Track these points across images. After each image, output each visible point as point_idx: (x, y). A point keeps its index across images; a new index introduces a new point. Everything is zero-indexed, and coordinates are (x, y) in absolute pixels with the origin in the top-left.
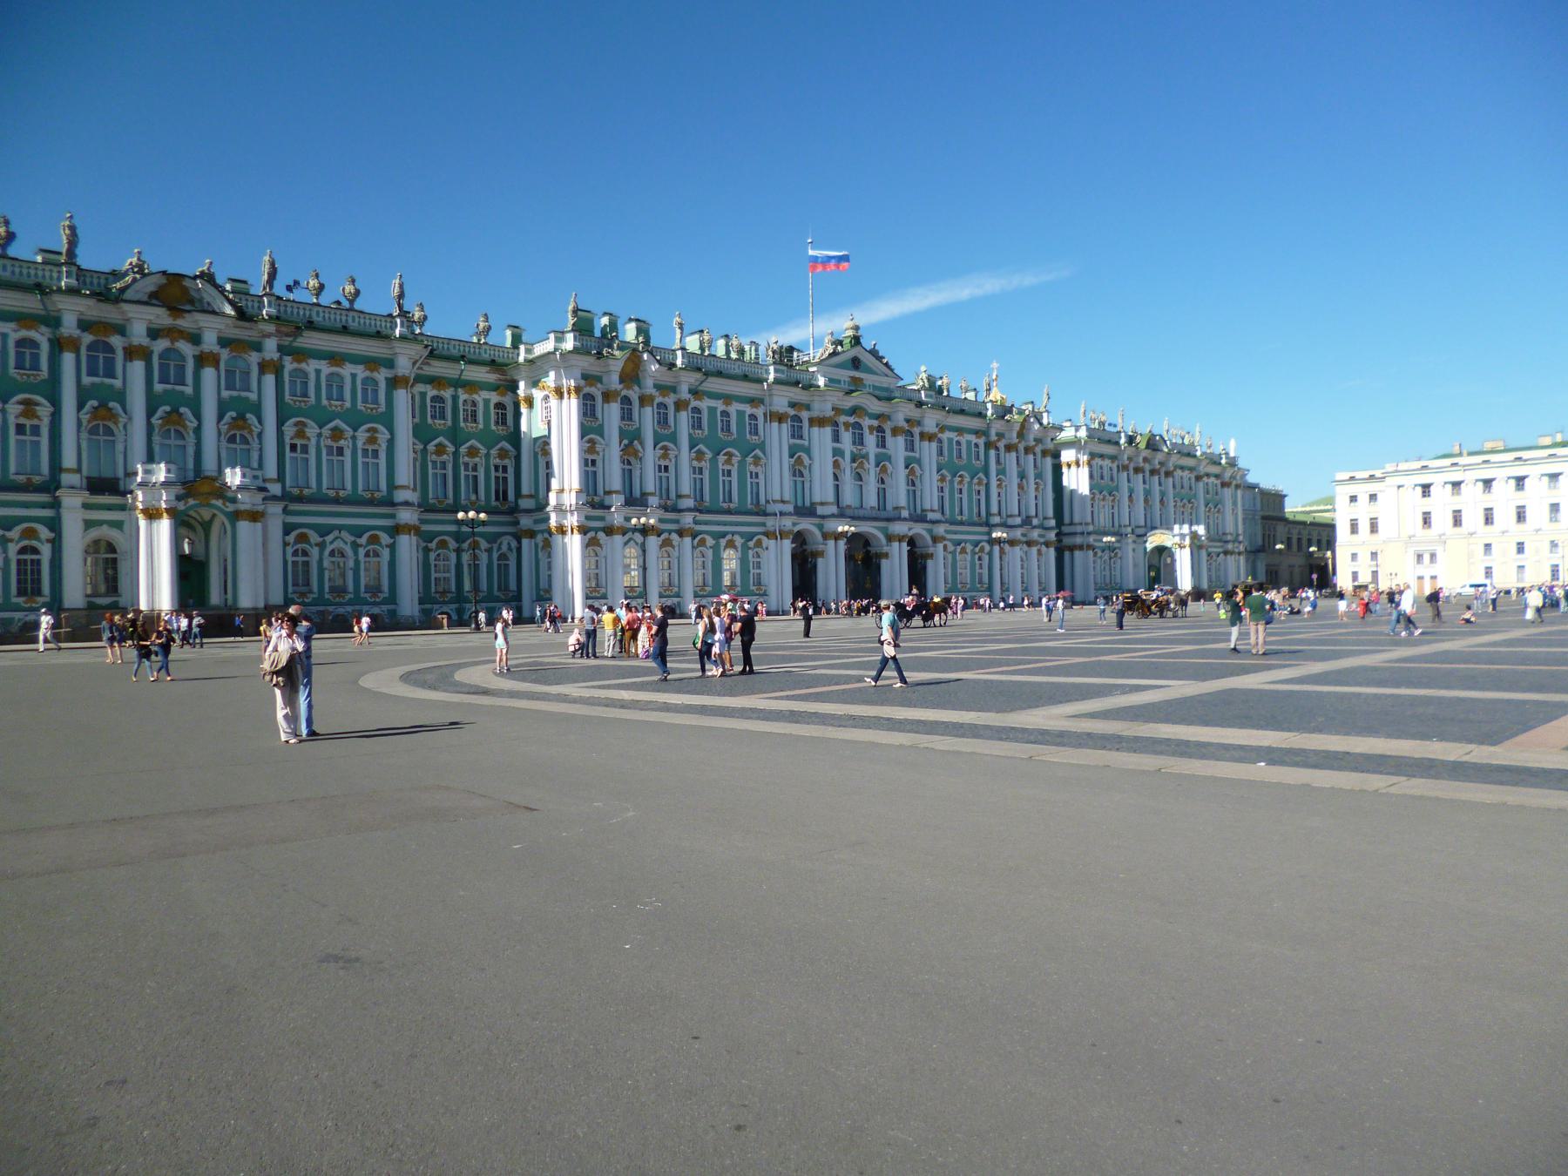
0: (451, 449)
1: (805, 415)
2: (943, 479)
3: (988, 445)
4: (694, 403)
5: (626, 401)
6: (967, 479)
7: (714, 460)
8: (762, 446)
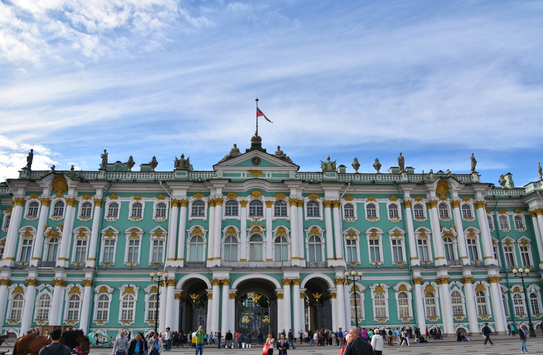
1: (205, 199)
3: (404, 205)
4: (109, 201)
7: (122, 234)
8: (166, 224)
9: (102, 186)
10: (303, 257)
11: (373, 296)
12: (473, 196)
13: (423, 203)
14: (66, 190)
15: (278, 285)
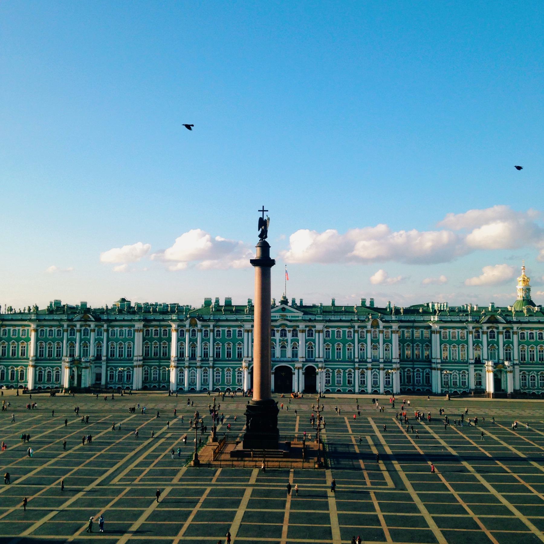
0: (158, 343)
2: (328, 345)
3: (355, 332)
4: (216, 329)
5: (194, 330)
6: (341, 345)
9: (213, 323)
10: (304, 356)
11: (336, 374)
12: (391, 327)
13: (365, 330)
14: (196, 325)
15: (293, 369)
